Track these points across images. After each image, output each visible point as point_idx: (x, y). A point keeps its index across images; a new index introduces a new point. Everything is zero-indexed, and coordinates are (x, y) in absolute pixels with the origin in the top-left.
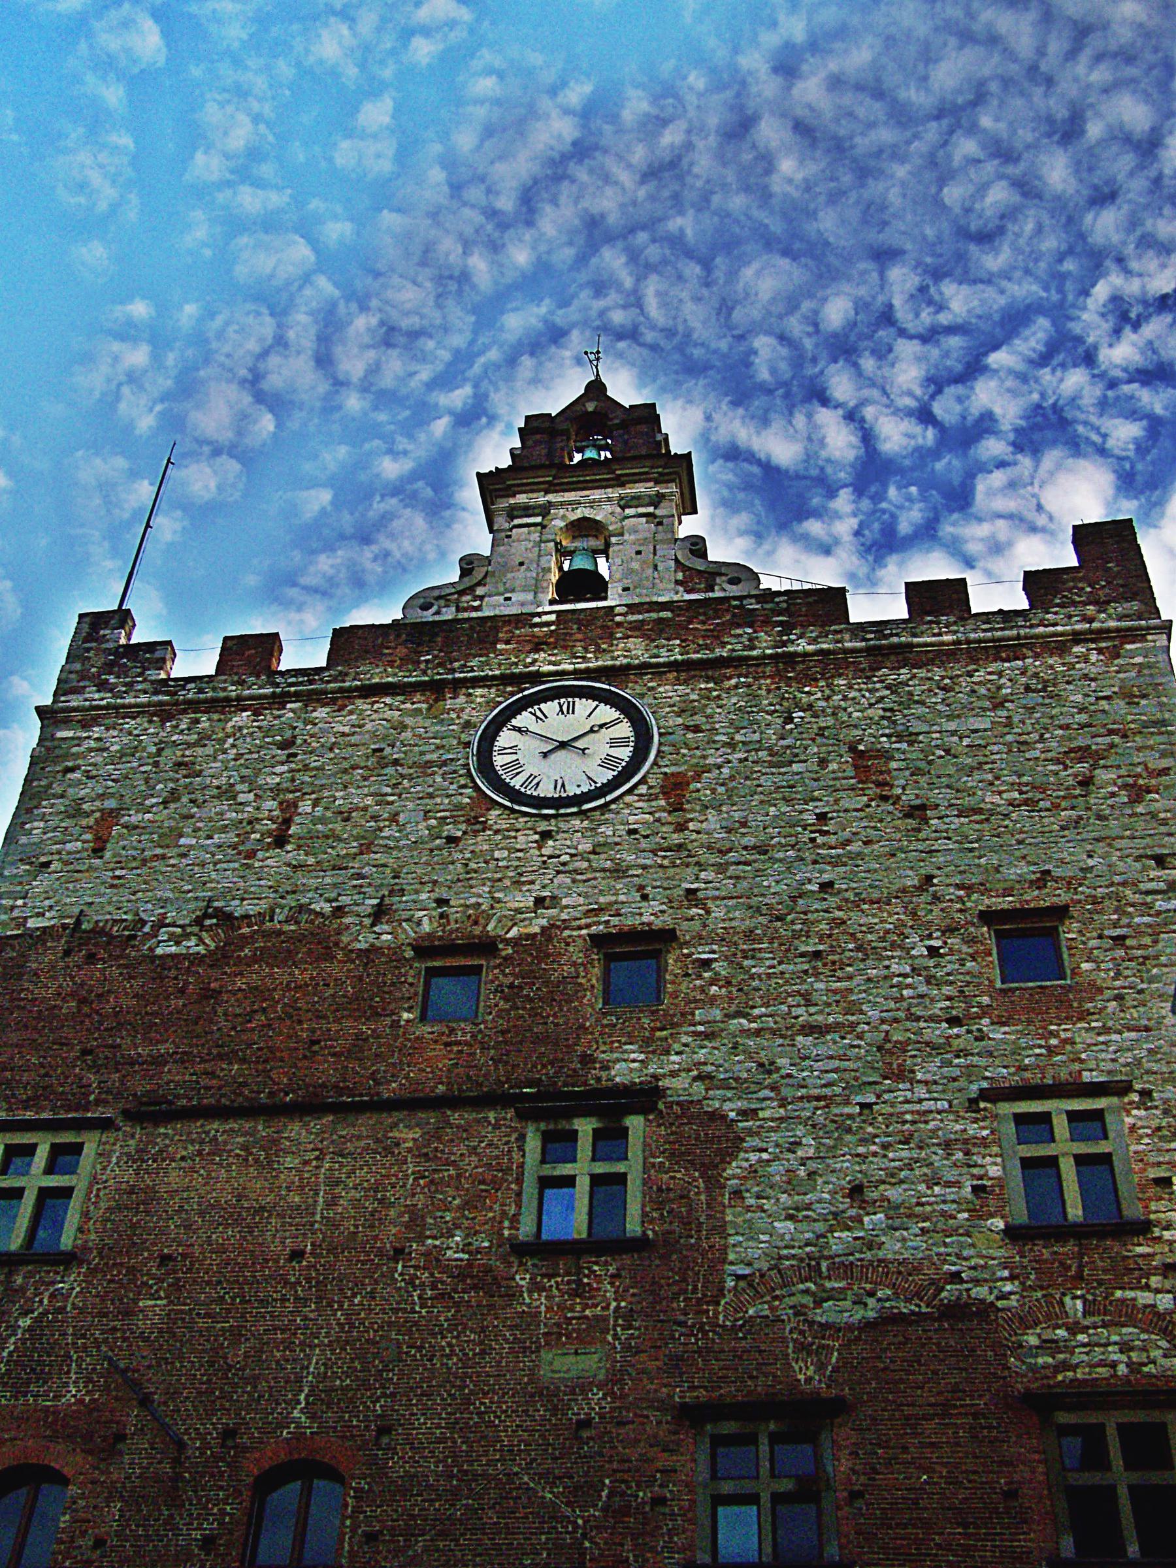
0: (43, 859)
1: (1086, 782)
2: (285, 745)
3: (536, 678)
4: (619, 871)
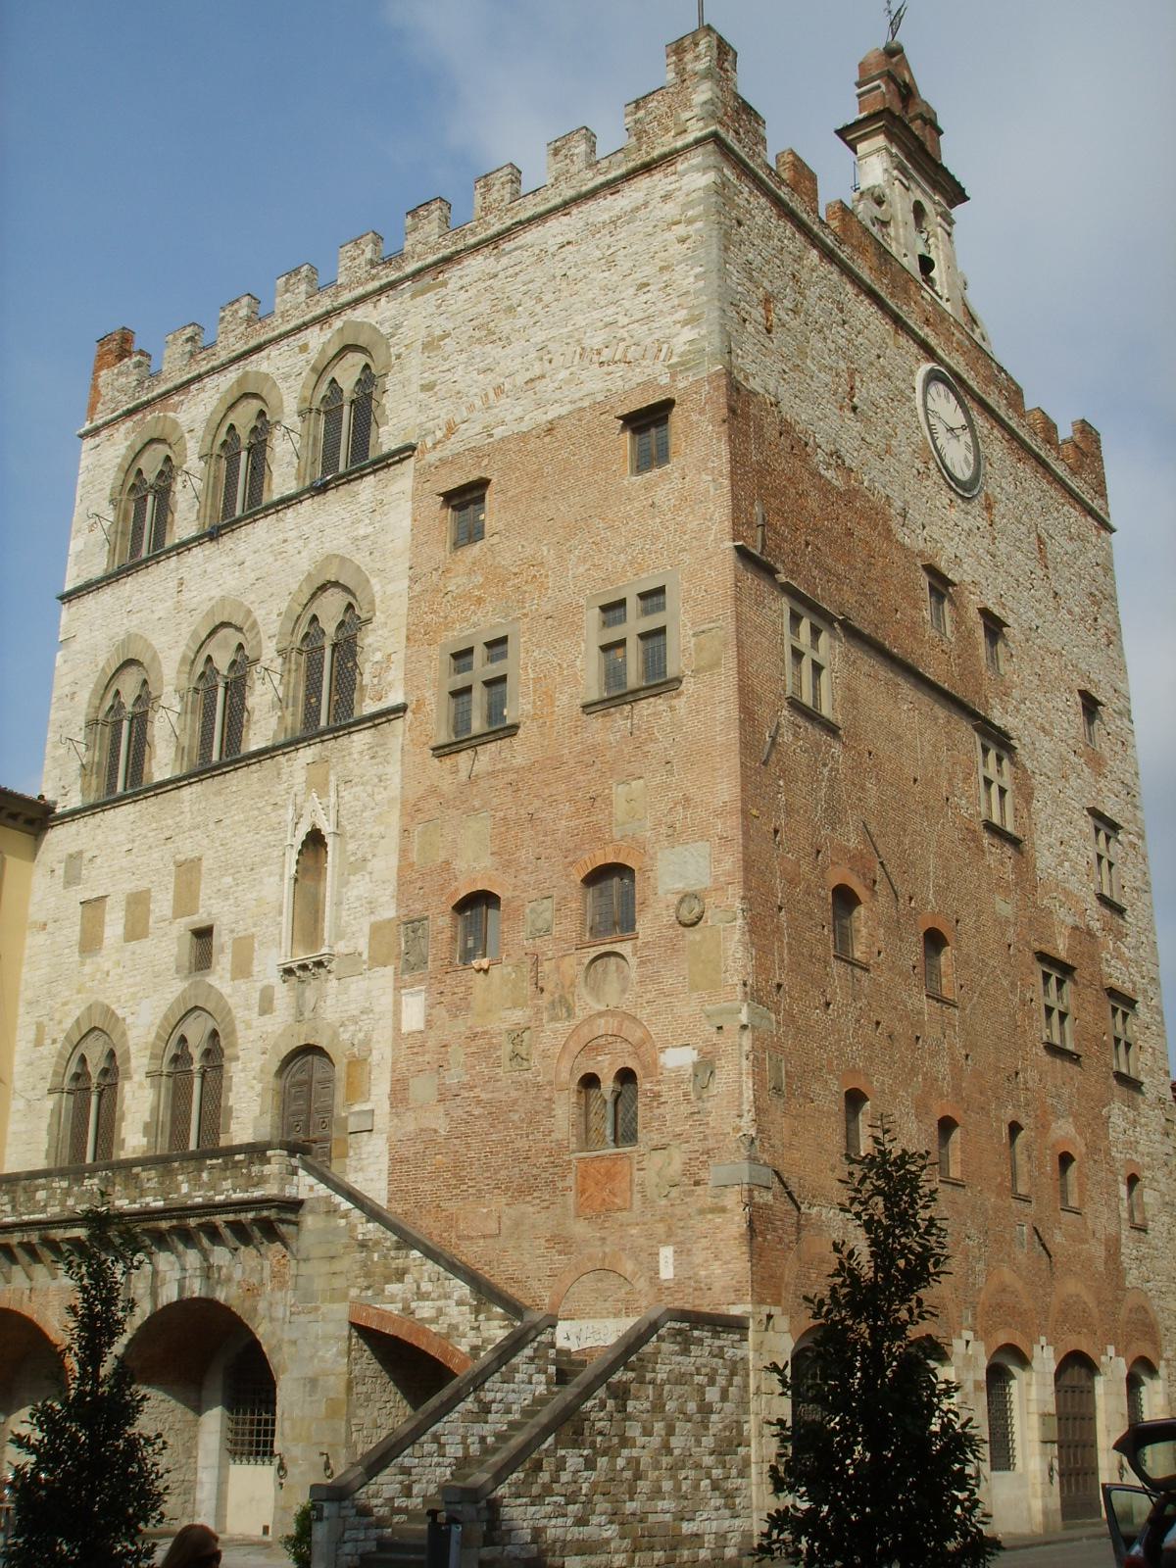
0: (743, 313)
1: (1096, 620)
2: (841, 310)
3: (930, 353)
4: (979, 558)
